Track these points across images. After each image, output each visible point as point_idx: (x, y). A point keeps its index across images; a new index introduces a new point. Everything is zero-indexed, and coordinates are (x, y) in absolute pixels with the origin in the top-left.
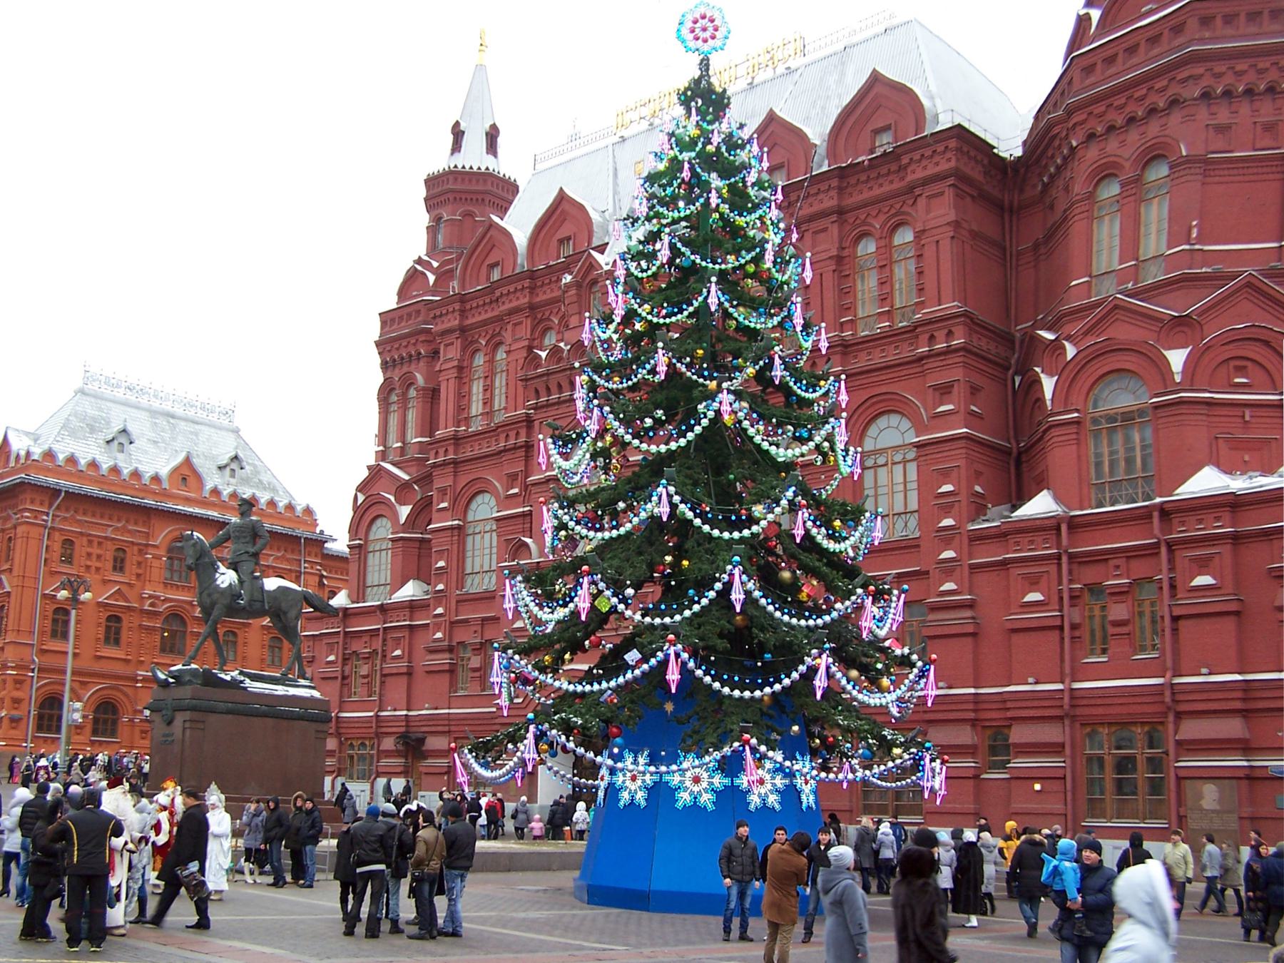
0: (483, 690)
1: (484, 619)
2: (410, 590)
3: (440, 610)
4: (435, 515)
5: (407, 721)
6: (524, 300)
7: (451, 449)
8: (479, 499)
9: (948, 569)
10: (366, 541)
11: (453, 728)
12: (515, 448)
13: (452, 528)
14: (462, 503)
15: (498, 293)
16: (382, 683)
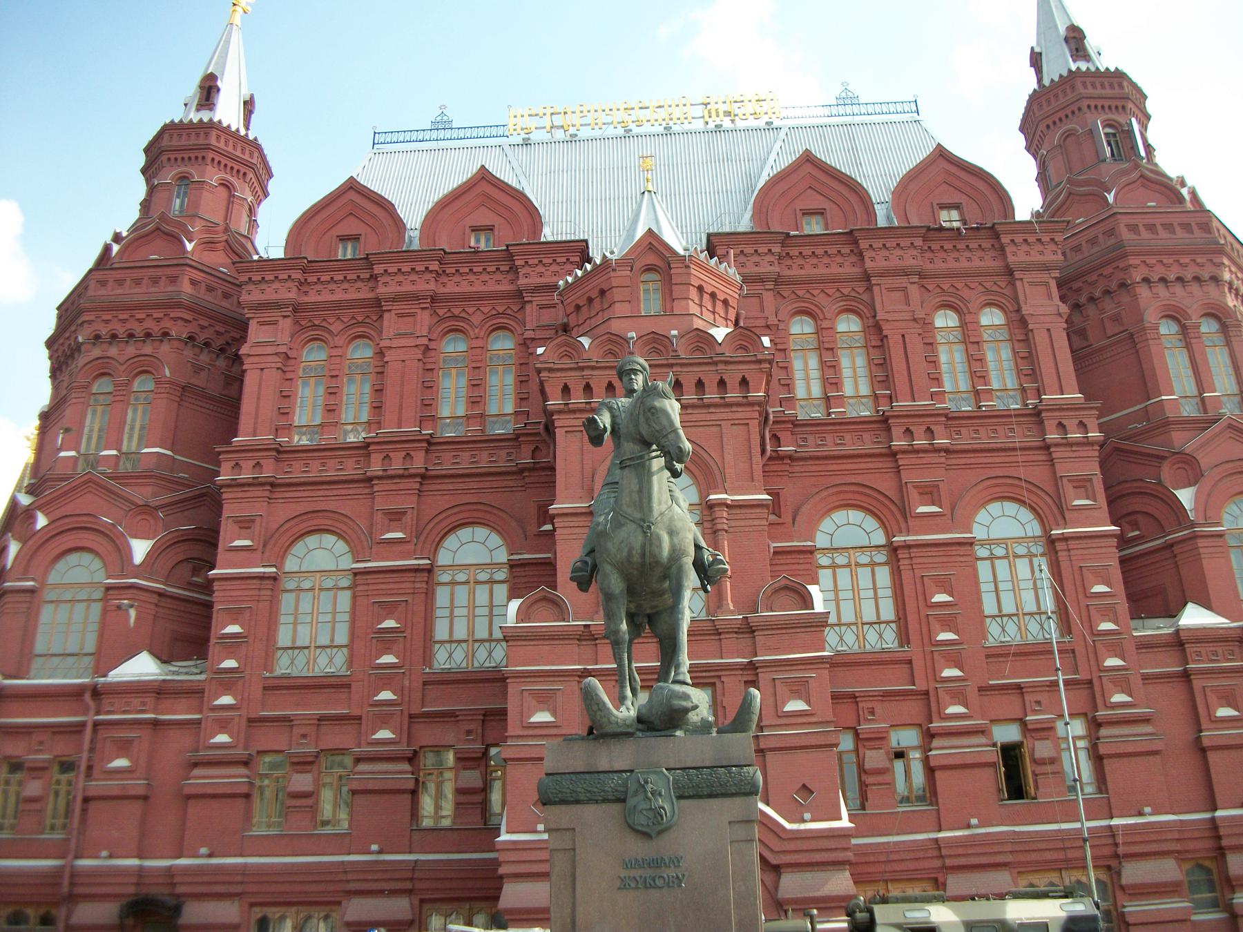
0: (315, 828)
1: (322, 719)
2: (142, 667)
3: (226, 700)
4: (221, 556)
5: (140, 876)
6: (426, 285)
7: (247, 465)
8: (312, 541)
9: (1121, 680)
10: (43, 584)
11: (418, 885)
12: (401, 476)
13: (262, 577)
14: (278, 543)
15: (378, 269)
16: (84, 811)
